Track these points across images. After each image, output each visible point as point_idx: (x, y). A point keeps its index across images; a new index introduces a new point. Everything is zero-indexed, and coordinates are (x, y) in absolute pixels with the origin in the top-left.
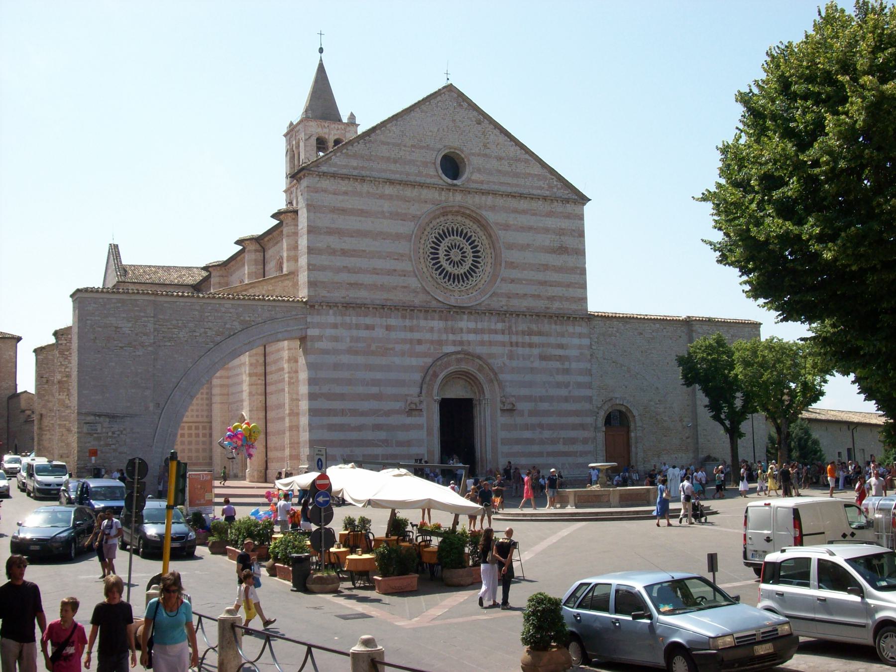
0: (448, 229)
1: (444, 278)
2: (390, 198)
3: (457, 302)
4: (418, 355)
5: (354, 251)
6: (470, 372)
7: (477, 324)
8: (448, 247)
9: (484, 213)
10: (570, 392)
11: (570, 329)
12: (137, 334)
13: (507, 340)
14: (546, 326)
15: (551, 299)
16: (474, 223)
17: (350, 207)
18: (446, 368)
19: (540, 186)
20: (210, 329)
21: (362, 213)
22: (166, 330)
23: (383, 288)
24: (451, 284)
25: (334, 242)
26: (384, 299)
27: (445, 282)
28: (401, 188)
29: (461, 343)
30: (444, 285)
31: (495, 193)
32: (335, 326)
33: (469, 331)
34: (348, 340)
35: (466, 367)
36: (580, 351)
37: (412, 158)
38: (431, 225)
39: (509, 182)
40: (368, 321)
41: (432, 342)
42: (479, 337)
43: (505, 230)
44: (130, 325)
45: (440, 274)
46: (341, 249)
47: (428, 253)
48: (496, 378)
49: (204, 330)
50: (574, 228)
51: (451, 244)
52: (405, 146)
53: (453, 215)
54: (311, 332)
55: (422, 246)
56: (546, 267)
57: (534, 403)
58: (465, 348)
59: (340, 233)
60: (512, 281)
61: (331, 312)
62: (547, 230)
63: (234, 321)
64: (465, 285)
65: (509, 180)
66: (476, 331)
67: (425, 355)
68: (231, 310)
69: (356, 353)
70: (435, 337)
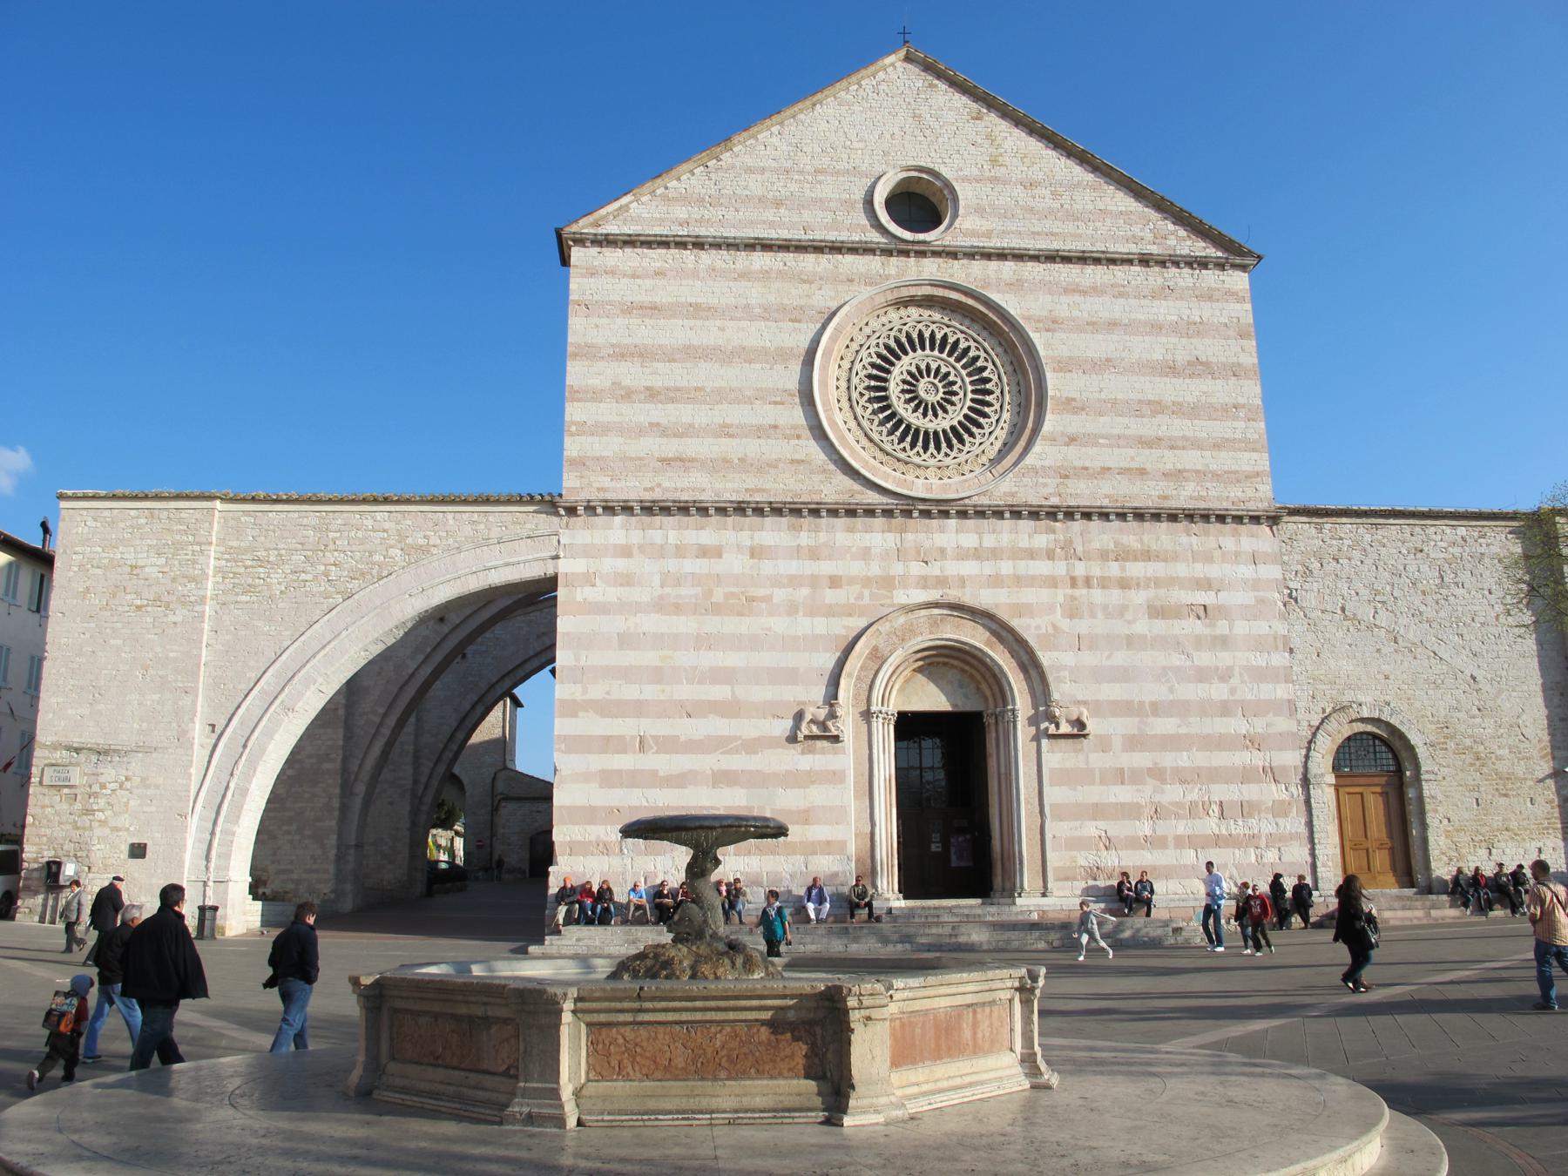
0: (908, 336)
1: (902, 440)
2: (765, 275)
3: (930, 489)
4: (830, 612)
5: (679, 389)
7: (981, 539)
8: (909, 373)
9: (995, 297)
10: (1233, 691)
11: (1229, 543)
12: (174, 580)
13: (1064, 573)
14: (1162, 535)
15: (1177, 475)
16: (973, 320)
17: (670, 300)
19: (1134, 236)
20: (335, 565)
21: (696, 311)
22: (242, 570)
23: (744, 465)
24: (918, 453)
25: (632, 374)
26: (747, 490)
27: (904, 450)
28: (791, 255)
29: (942, 582)
30: (902, 455)
31: (1019, 256)
32: (626, 552)
33: (963, 555)
34: (656, 581)
36: (1256, 593)
37: (820, 195)
38: (867, 331)
39: (1057, 230)
40: (708, 532)
41: (866, 582)
42: (988, 568)
43: (1047, 330)
44: (162, 561)
45: (891, 433)
46: (648, 388)
47: (860, 389)
49: (323, 568)
50: (1222, 320)
51: (918, 368)
52: (801, 172)
53: (920, 306)
54: (564, 567)
55: (844, 376)
56: (1157, 407)
57: (1137, 719)
58: (954, 595)
59: (643, 354)
60: (1072, 440)
61: (618, 520)
62: (1156, 327)
63: (392, 547)
64: (953, 454)
65: (1057, 226)
66: (977, 554)
67: (849, 611)
68: (387, 526)
69: (678, 609)
70: (875, 569)
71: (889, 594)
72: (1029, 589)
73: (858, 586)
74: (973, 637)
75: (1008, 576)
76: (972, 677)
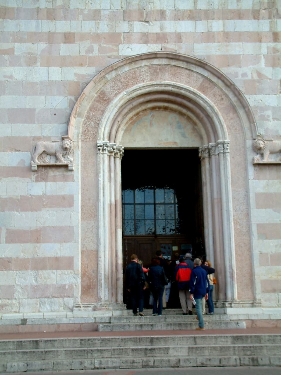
6: (183, 92)
18: (127, 86)
29: (161, 38)
35: (172, 83)
41: (97, 37)
42: (201, 26)
48: (241, 102)
58: (172, 47)
70: (104, 28)
71: (115, 48)
72: (237, 44)
73: (88, 42)
74: (188, 83)
75: (219, 33)
76: (189, 118)
